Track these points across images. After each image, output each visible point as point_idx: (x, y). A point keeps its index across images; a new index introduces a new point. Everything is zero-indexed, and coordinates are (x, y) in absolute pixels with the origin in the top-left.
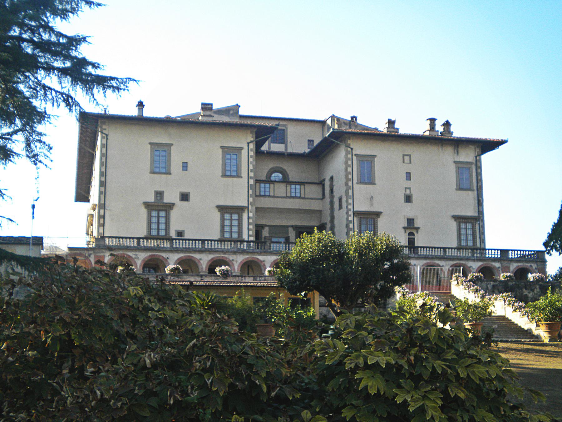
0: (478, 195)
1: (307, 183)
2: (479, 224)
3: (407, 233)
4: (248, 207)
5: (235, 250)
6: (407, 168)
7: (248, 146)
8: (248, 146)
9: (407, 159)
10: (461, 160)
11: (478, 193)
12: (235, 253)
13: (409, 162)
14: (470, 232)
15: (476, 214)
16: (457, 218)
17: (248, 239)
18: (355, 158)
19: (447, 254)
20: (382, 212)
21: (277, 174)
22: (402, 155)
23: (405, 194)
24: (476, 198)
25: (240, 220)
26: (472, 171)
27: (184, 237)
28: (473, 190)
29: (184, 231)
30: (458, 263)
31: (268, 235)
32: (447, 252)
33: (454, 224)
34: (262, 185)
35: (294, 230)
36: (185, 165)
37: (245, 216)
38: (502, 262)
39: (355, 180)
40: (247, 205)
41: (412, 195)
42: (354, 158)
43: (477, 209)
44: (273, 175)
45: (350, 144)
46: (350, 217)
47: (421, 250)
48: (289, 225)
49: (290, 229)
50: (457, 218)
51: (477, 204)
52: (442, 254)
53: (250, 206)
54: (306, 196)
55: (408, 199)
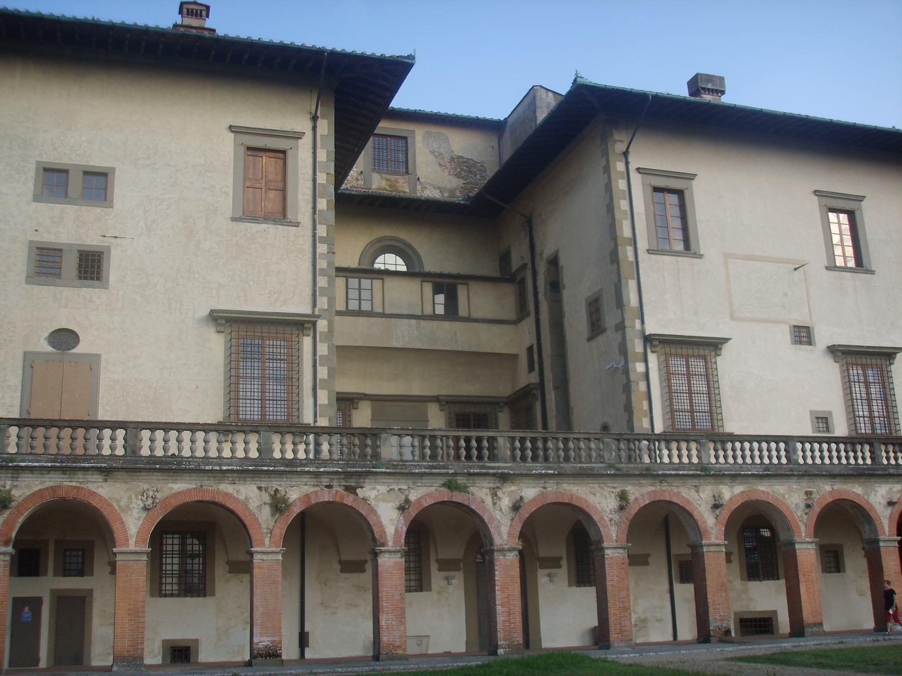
17: (315, 421)
18: (635, 178)
20: (727, 340)
34: (353, 282)
42: (635, 178)
44: (380, 259)
54: (474, 315)
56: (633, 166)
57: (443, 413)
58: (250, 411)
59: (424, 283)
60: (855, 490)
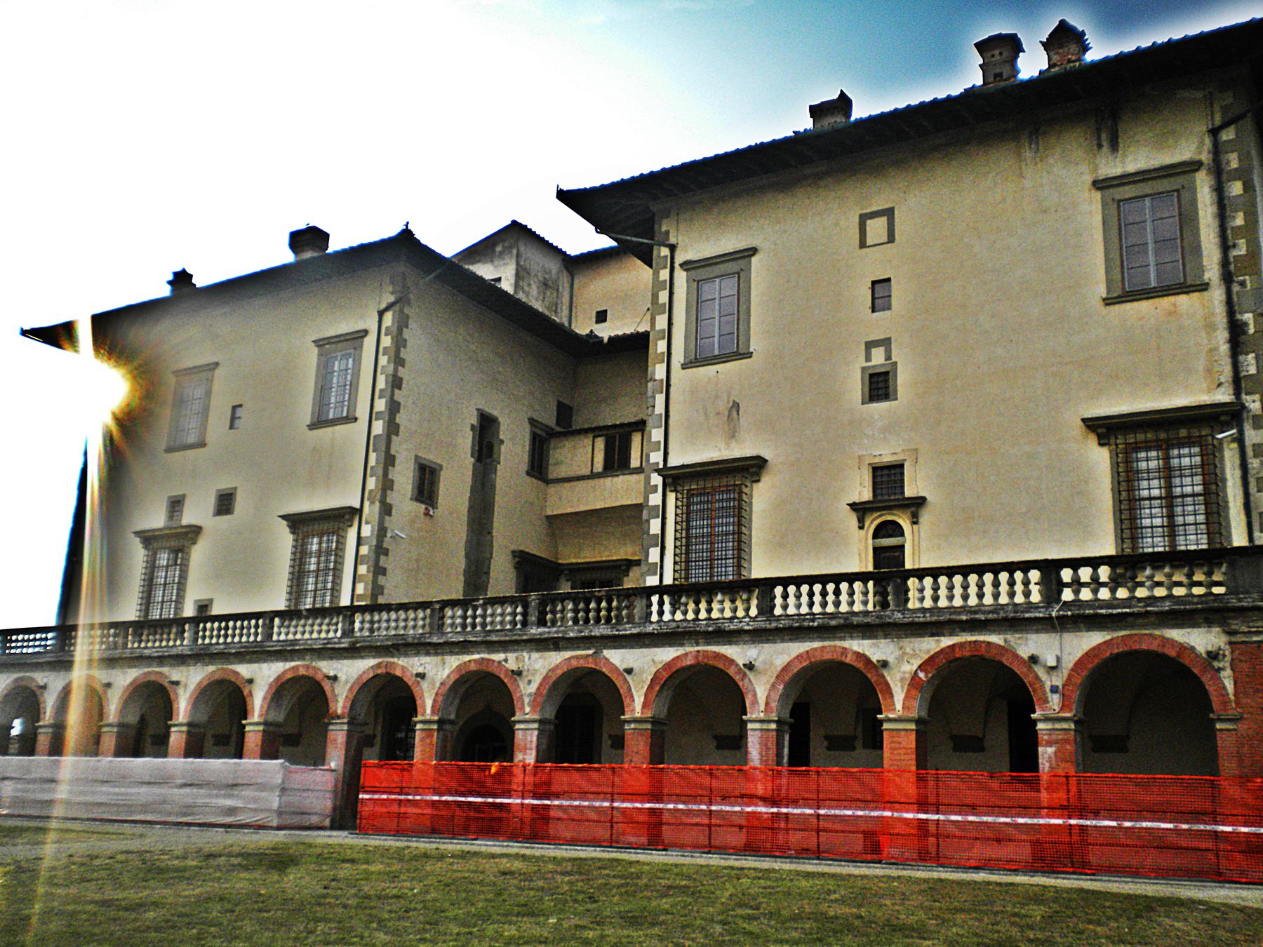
2: (1240, 440)
3: (871, 525)
4: (360, 511)
6: (874, 265)
9: (877, 228)
10: (1131, 167)
14: (1191, 485)
15: (1224, 396)
18: (681, 277)
23: (863, 369)
26: (1194, 202)
28: (1204, 287)
30: (962, 645)
38: (1236, 625)
39: (678, 357)
42: (681, 277)
43: (1227, 370)
45: (667, 233)
46: (651, 496)
47: (785, 596)
51: (1224, 348)
53: (367, 504)
60: (408, 665)
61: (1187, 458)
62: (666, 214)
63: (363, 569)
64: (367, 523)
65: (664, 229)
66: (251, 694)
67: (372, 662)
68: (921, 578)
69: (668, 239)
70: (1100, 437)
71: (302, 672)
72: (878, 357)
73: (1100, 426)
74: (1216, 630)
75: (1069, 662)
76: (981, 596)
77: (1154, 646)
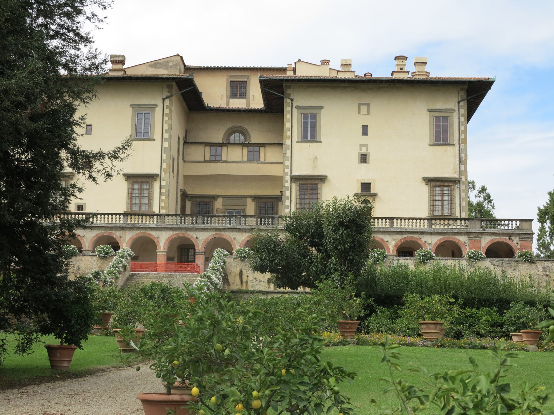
0: (459, 150)
1: (266, 144)
2: (460, 188)
5: (124, 225)
6: (364, 120)
7: (163, 103)
8: (163, 103)
11: (460, 147)
12: (123, 228)
13: (366, 113)
14: (447, 198)
15: (457, 176)
16: (429, 181)
18: (295, 111)
19: (395, 226)
21: (237, 135)
22: (358, 104)
23: (359, 153)
24: (458, 155)
25: (150, 190)
27: (85, 211)
28: (453, 145)
29: (85, 203)
30: (407, 237)
31: (221, 207)
32: (395, 224)
33: (425, 189)
35: (253, 200)
36: (89, 127)
37: (156, 185)
40: (159, 173)
41: (369, 153)
42: (295, 111)
44: (233, 136)
45: (290, 94)
46: (286, 183)
48: (249, 195)
49: (249, 200)
50: (429, 181)
51: (458, 163)
52: (388, 226)
53: (163, 173)
54: (267, 160)
55: (364, 158)
56: (294, 105)
57: (254, 202)
58: (136, 209)
59: (244, 147)
61: (446, 190)
62: (289, 87)
63: (163, 198)
64: (163, 180)
65: (288, 92)
66: (158, 242)
67: (213, 233)
68: (397, 220)
69: (290, 96)
70: (426, 182)
71: (181, 235)
72: (364, 150)
73: (427, 180)
74: (466, 237)
75: (434, 242)
76: (412, 225)
77: (453, 240)
